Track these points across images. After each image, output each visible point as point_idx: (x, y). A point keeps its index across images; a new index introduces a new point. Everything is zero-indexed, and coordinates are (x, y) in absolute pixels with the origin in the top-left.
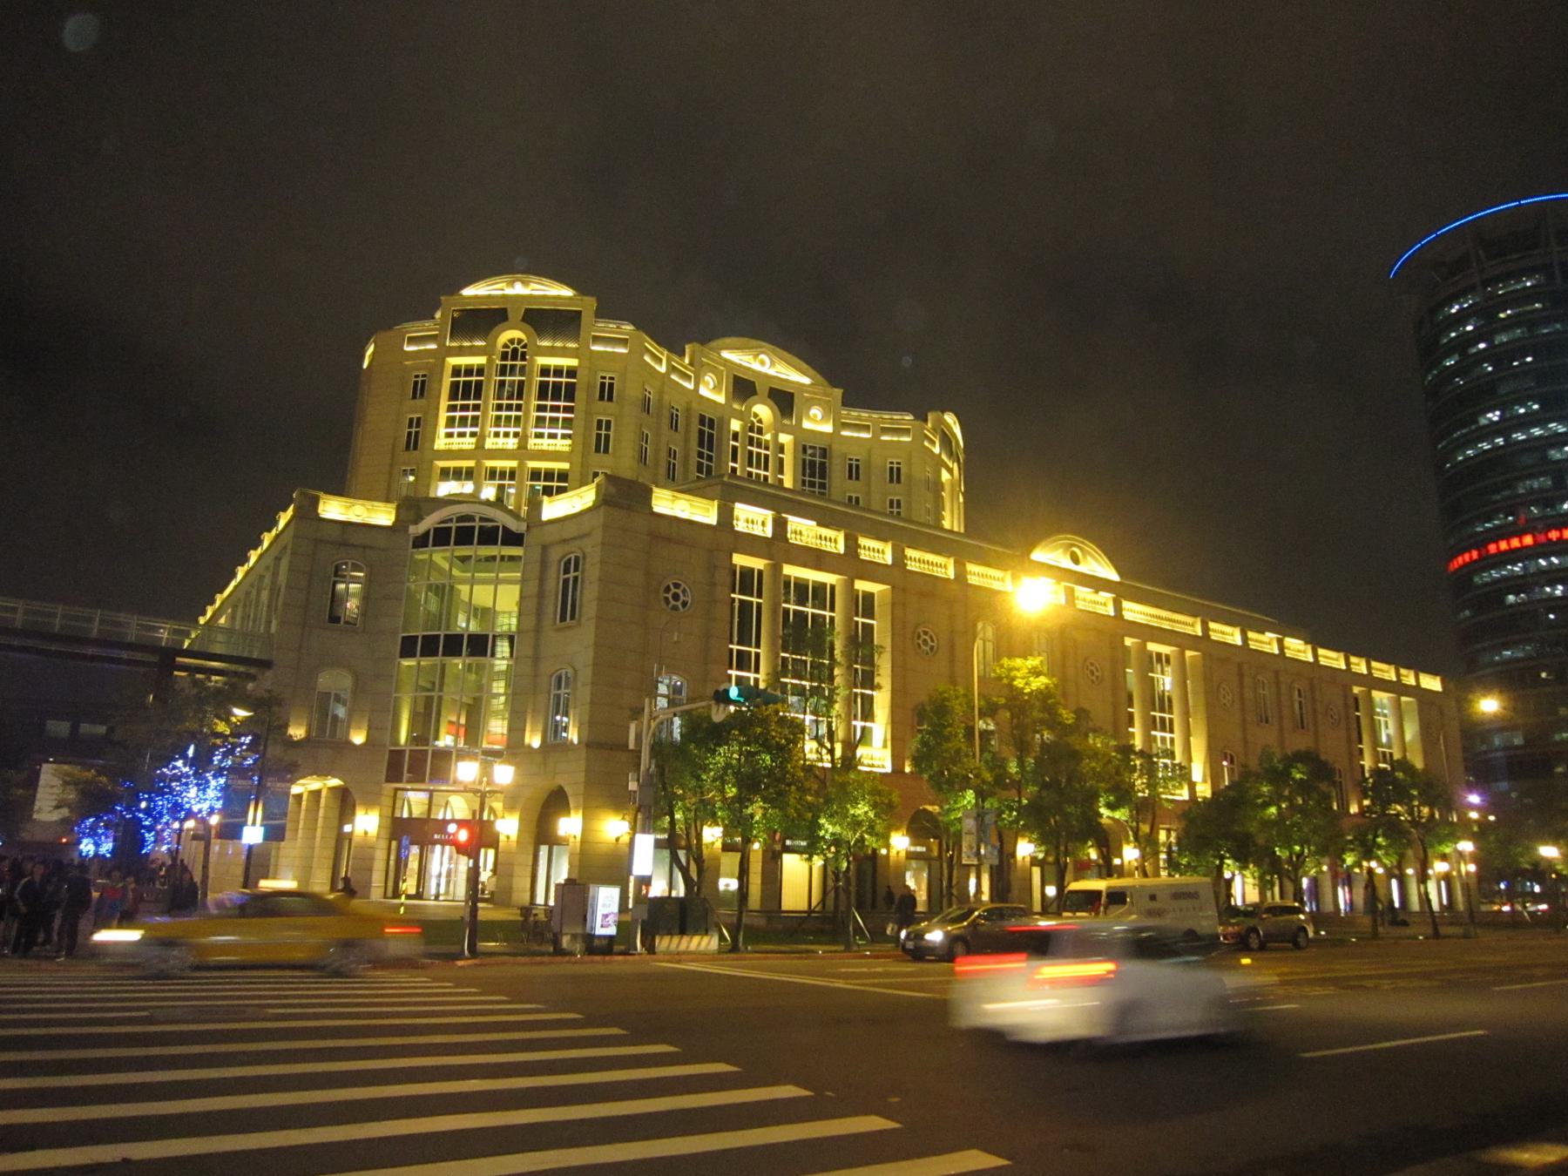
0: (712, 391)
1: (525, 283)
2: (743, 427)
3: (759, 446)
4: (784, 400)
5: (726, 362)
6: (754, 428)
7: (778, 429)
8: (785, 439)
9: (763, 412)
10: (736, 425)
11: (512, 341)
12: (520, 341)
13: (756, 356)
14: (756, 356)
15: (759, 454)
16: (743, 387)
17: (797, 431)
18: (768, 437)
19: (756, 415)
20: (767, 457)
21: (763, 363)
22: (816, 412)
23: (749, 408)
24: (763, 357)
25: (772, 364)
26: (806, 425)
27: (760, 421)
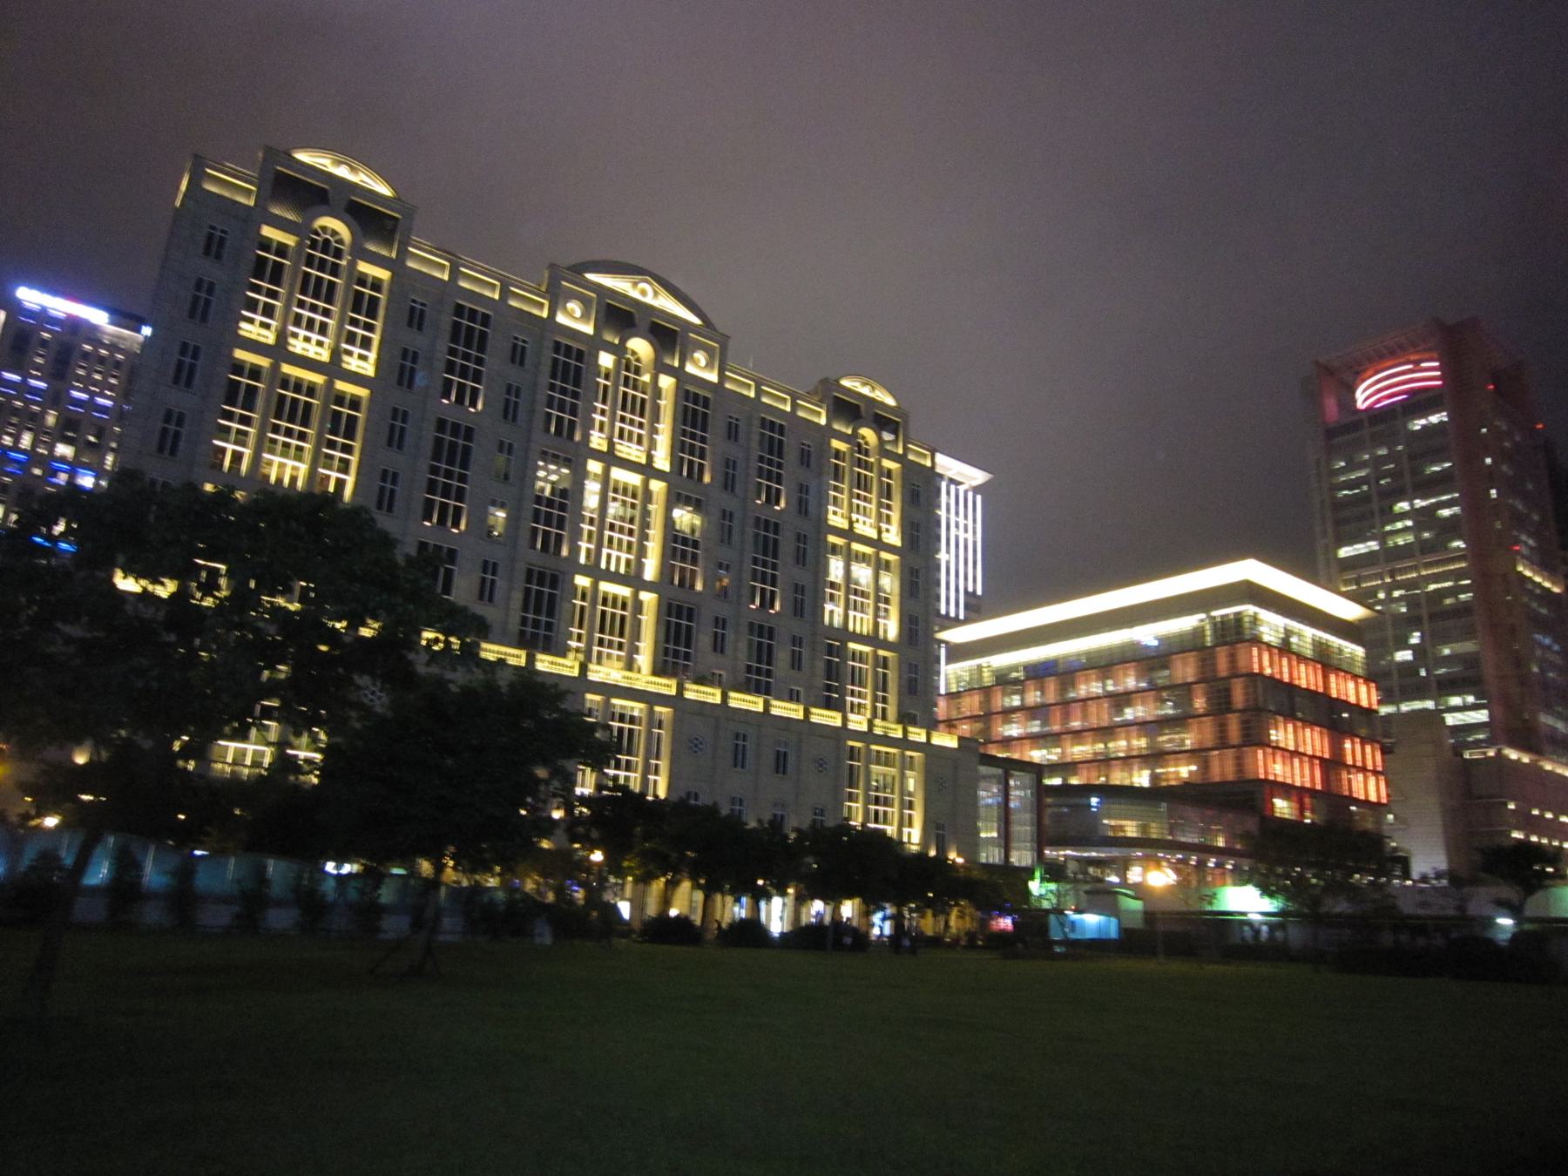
0: (574, 318)
1: (353, 169)
2: (617, 363)
3: (635, 388)
4: (666, 336)
5: (599, 288)
6: (628, 366)
7: (660, 367)
8: (666, 382)
9: (640, 347)
10: (606, 360)
11: (324, 229)
12: (334, 233)
13: (635, 284)
14: (635, 284)
15: (634, 397)
16: (620, 317)
17: (678, 373)
18: (646, 378)
19: (634, 353)
20: (643, 400)
21: (644, 293)
22: (700, 356)
23: (623, 341)
24: (643, 285)
25: (656, 294)
26: (690, 368)
27: (638, 360)
